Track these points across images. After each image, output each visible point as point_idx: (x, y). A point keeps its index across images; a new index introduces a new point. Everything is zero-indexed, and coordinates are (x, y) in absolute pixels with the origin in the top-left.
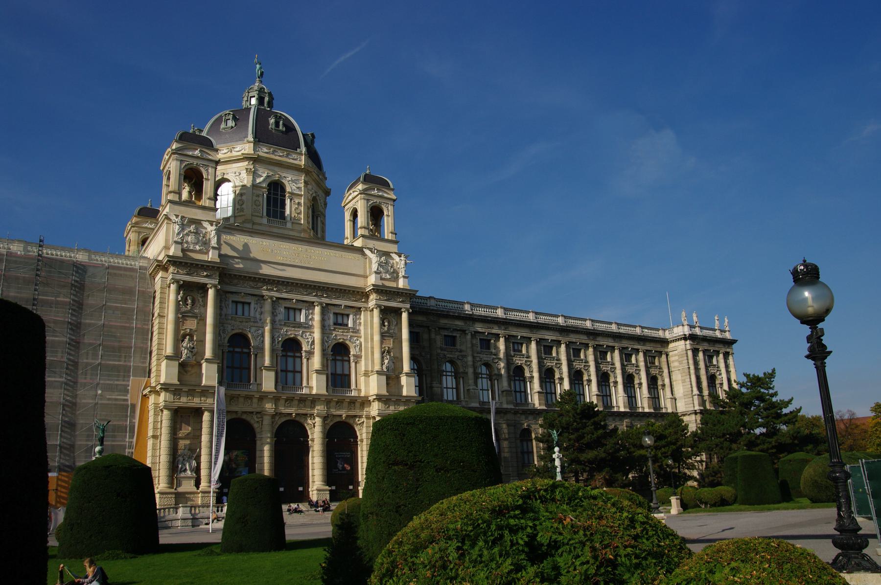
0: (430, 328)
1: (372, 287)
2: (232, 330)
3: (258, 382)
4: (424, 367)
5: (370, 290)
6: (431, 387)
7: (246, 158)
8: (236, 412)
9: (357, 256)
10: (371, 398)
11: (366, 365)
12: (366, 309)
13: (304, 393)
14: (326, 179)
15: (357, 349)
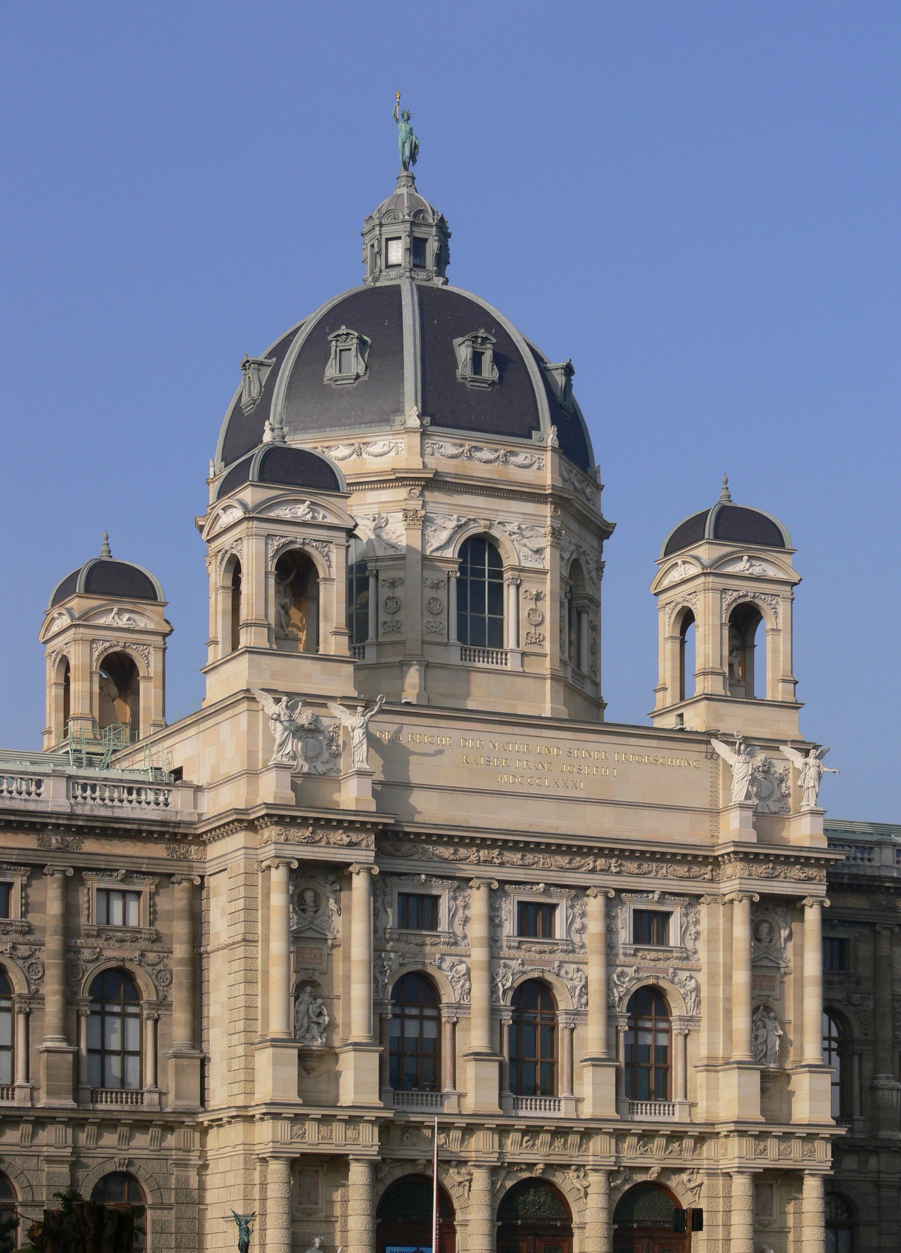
0: (878, 928)
1: (732, 849)
2: (402, 965)
3: (459, 1090)
4: (857, 1034)
5: (728, 854)
6: (874, 1089)
7: (399, 480)
8: (414, 1161)
9: (692, 754)
10: (723, 1129)
11: (711, 1043)
12: (716, 897)
13: (561, 1115)
14: (600, 488)
15: (690, 1002)
